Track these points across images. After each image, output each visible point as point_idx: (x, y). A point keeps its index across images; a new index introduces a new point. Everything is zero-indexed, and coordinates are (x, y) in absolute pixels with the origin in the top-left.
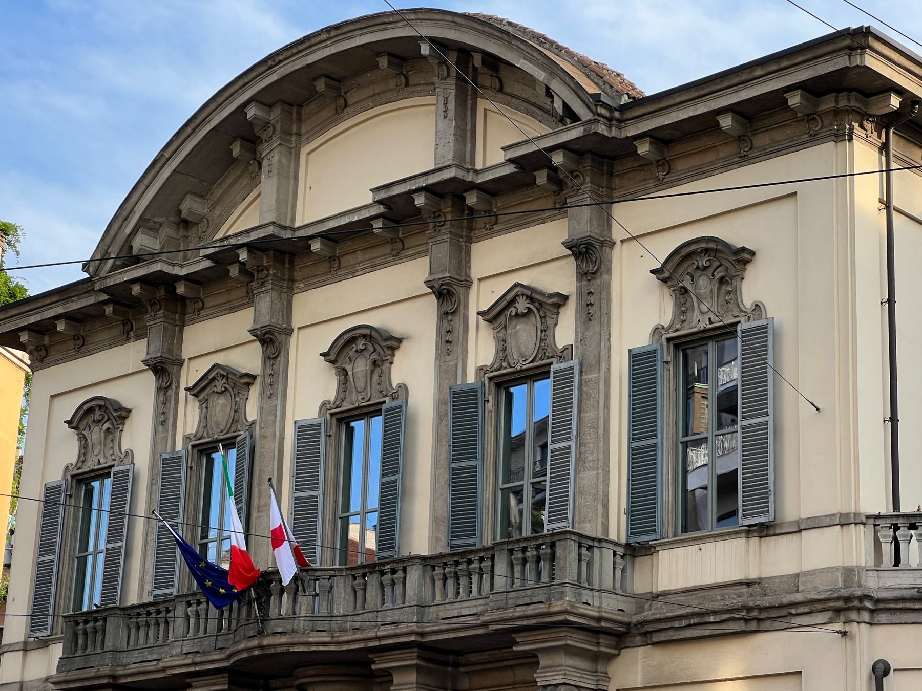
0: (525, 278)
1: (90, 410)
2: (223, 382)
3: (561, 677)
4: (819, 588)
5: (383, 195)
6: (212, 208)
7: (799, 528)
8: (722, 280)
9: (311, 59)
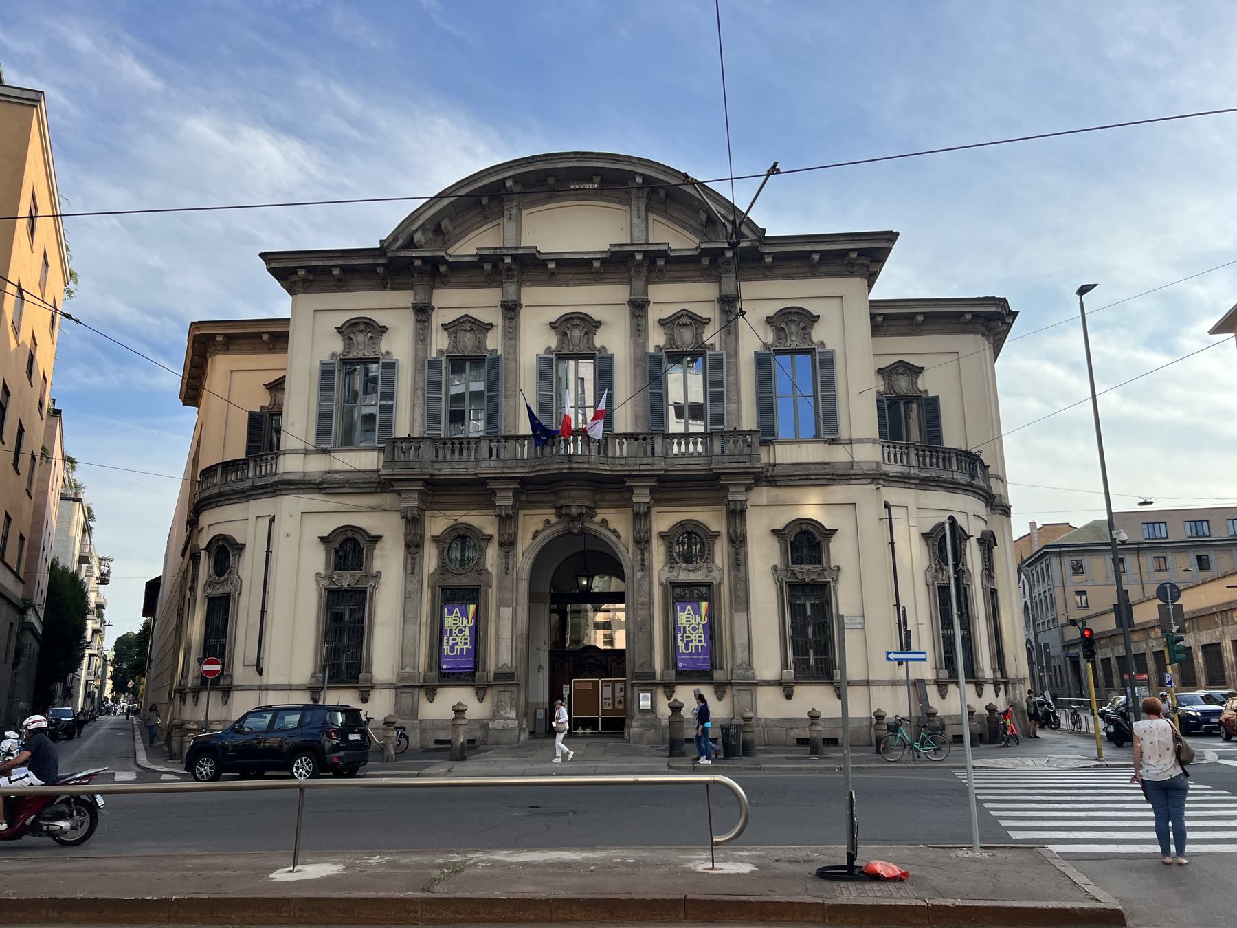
0: (688, 307)
1: (357, 324)
2: (465, 325)
4: (866, 468)
5: (614, 249)
6: (454, 228)
7: (851, 442)
8: (804, 328)
9: (559, 165)
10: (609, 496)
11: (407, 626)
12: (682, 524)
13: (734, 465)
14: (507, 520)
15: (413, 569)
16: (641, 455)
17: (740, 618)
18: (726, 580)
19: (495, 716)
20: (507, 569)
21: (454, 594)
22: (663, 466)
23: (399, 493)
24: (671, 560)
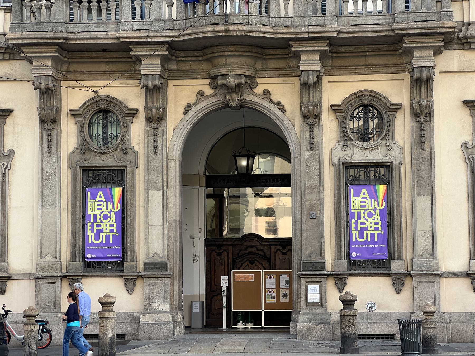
3: (432, 63)
10: (272, 64)
11: (46, 211)
12: (357, 95)
13: (420, 25)
14: (154, 91)
15: (50, 147)
16: (310, 14)
17: (423, 203)
18: (408, 159)
19: (146, 310)
20: (155, 147)
21: (99, 176)
22: (336, 27)
23: (30, 60)
24: (345, 138)
